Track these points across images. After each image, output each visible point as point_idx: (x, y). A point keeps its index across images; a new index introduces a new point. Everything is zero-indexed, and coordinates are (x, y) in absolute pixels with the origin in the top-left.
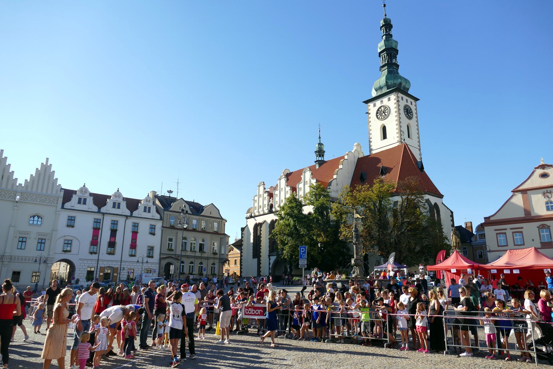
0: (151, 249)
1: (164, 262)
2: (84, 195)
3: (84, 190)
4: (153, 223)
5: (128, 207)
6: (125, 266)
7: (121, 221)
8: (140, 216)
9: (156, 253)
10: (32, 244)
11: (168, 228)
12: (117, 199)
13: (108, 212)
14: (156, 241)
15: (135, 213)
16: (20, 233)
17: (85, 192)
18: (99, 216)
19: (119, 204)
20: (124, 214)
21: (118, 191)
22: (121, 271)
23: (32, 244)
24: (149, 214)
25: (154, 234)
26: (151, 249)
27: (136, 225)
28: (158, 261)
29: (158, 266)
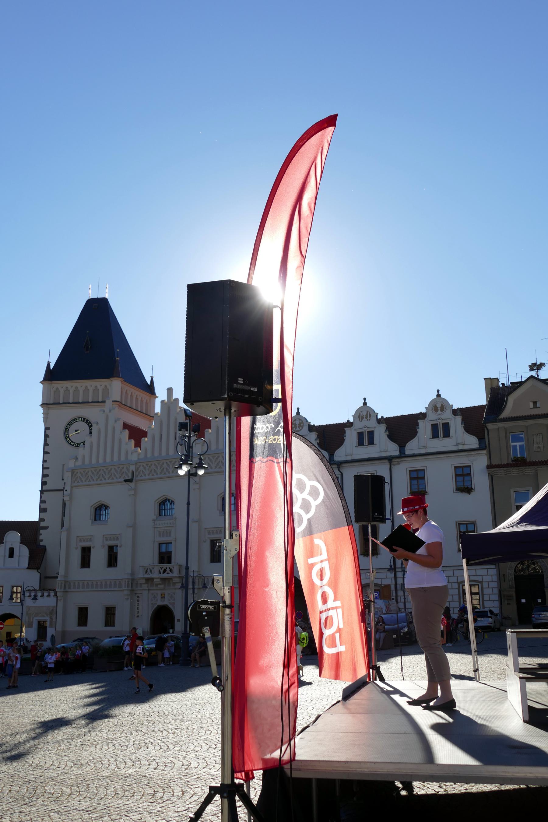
4: (462, 460)
5: (391, 437)
8: (423, 451)
10: (99, 556)
11: (507, 466)
12: (365, 422)
13: (349, 458)
15: (412, 447)
16: (209, 533)
17: (300, 424)
19: (371, 434)
20: (384, 455)
21: (365, 404)
23: (99, 556)
24: (447, 440)
25: (468, 490)
27: (417, 477)
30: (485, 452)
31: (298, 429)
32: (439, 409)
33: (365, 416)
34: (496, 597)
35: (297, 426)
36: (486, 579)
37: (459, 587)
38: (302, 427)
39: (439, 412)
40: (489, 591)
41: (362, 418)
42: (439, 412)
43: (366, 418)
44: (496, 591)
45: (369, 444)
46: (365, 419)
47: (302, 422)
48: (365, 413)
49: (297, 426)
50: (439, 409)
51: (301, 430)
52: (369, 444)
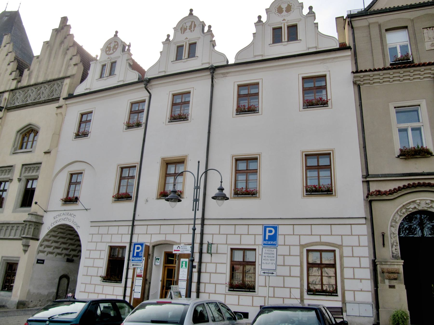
0: (318, 163)
1: (391, 214)
2: (112, 56)
3: (112, 45)
4: (313, 69)
6: (218, 239)
7: (199, 88)
8: (260, 58)
9: (348, 175)
14: (336, 127)
18: (140, 94)
22: (206, 257)
26: (318, 163)
28: (360, 210)
29: (364, 229)
30: (348, 53)
31: (111, 52)
32: (284, 10)
33: (188, 28)
34: (367, 274)
35: (112, 49)
36: (347, 241)
37: (301, 253)
38: (116, 49)
39: (284, 13)
40: (355, 262)
41: (185, 29)
42: (284, 13)
43: (190, 29)
44: (367, 263)
45: (189, 57)
46: (188, 30)
47: (118, 44)
48: (188, 24)
49: (112, 49)
50: (284, 10)
51: (114, 52)
52: (189, 57)
